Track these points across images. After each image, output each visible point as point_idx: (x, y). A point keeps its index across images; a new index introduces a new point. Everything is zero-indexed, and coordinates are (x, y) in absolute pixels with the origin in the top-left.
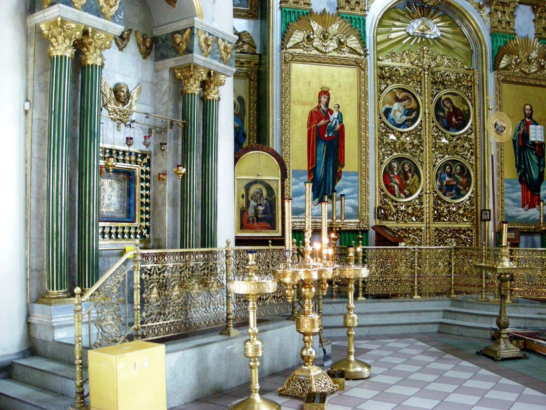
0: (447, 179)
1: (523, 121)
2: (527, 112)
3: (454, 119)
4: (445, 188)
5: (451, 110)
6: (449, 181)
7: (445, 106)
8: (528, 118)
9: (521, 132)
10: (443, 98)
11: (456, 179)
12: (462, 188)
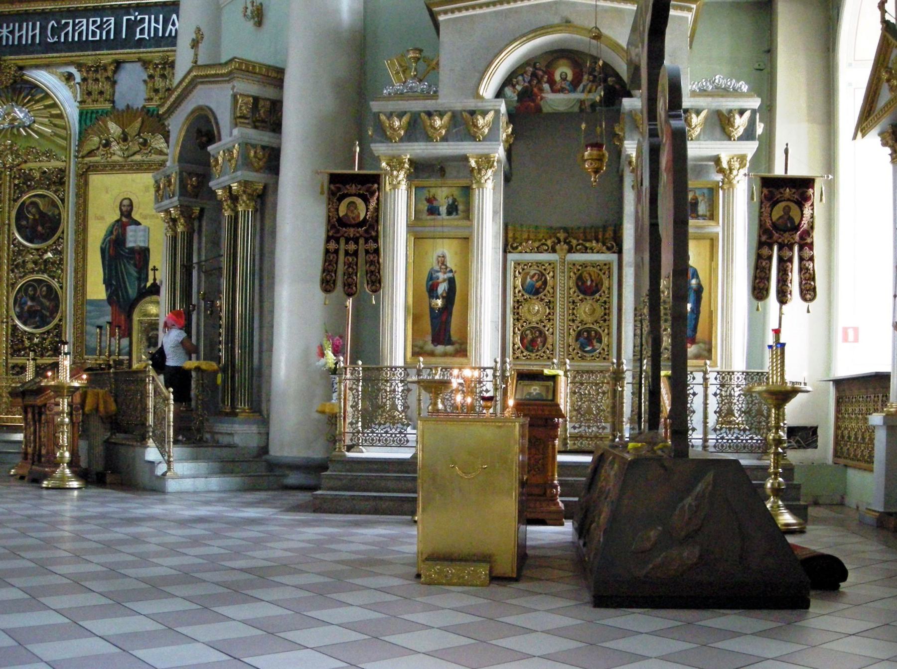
0: (29, 303)
1: (117, 221)
2: (124, 209)
3: (40, 228)
4: (26, 315)
5: (37, 217)
6: (31, 307)
7: (29, 212)
8: (126, 217)
9: (113, 237)
10: (27, 202)
11: (42, 304)
12: (48, 314)
